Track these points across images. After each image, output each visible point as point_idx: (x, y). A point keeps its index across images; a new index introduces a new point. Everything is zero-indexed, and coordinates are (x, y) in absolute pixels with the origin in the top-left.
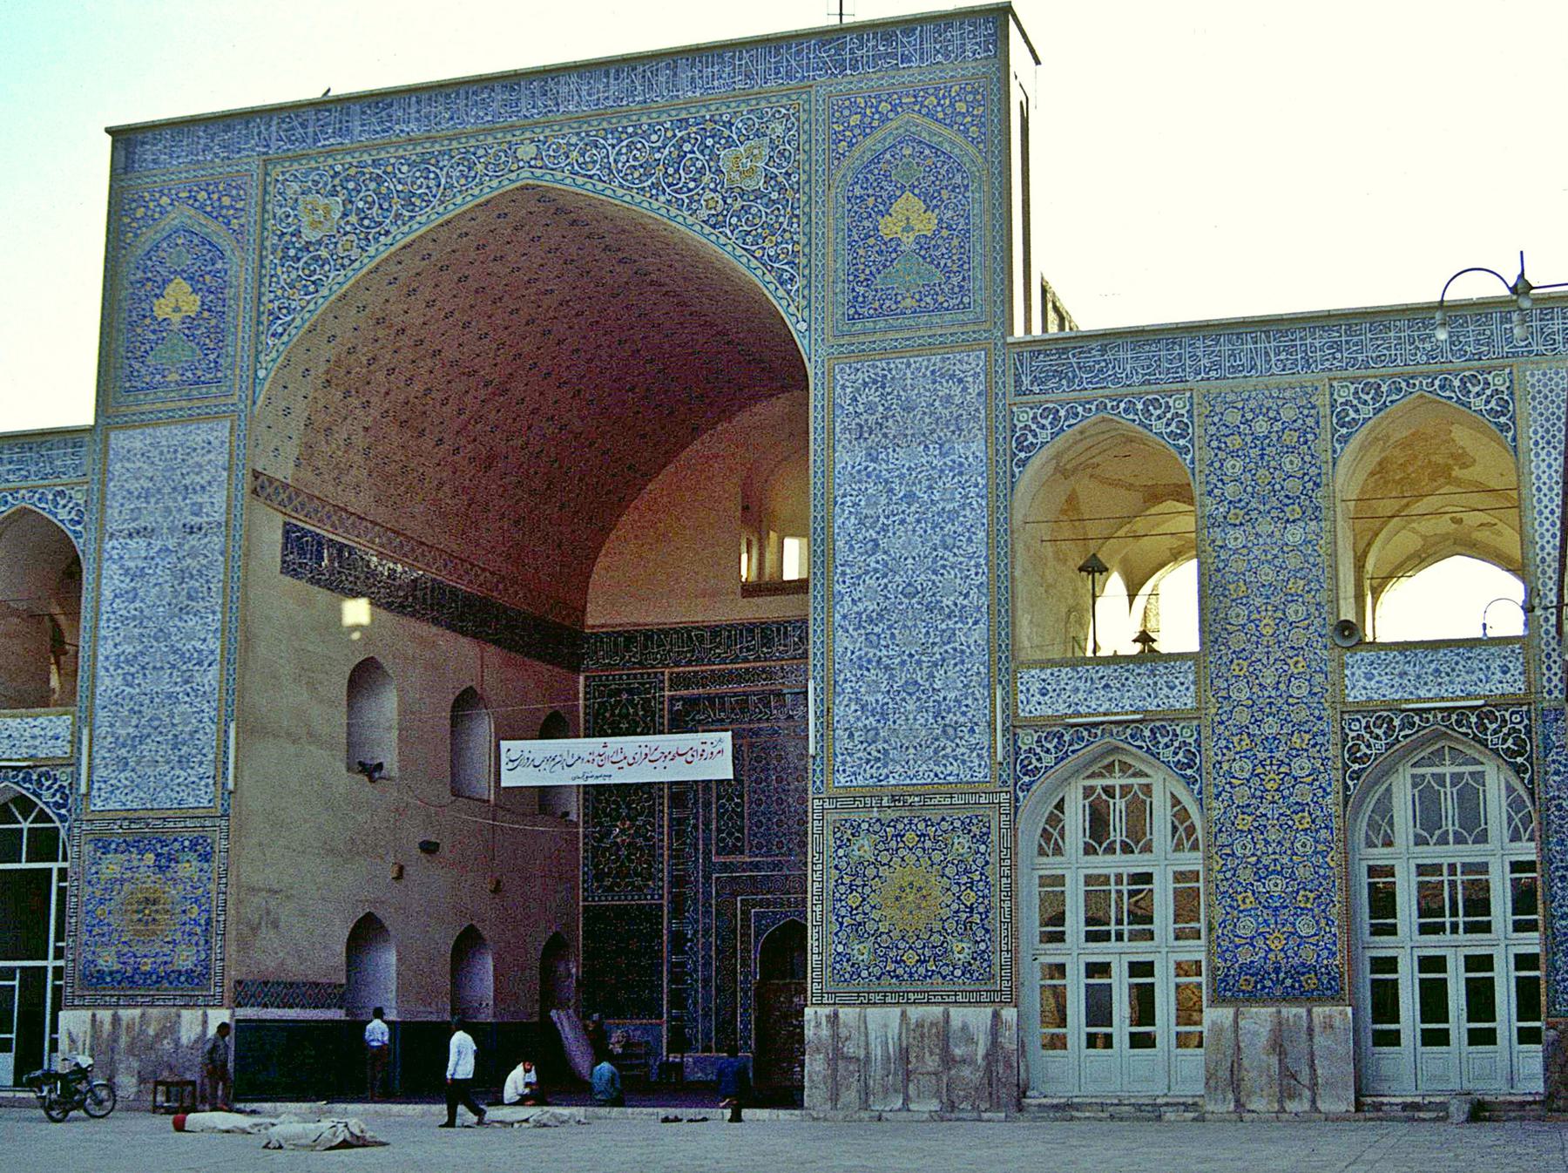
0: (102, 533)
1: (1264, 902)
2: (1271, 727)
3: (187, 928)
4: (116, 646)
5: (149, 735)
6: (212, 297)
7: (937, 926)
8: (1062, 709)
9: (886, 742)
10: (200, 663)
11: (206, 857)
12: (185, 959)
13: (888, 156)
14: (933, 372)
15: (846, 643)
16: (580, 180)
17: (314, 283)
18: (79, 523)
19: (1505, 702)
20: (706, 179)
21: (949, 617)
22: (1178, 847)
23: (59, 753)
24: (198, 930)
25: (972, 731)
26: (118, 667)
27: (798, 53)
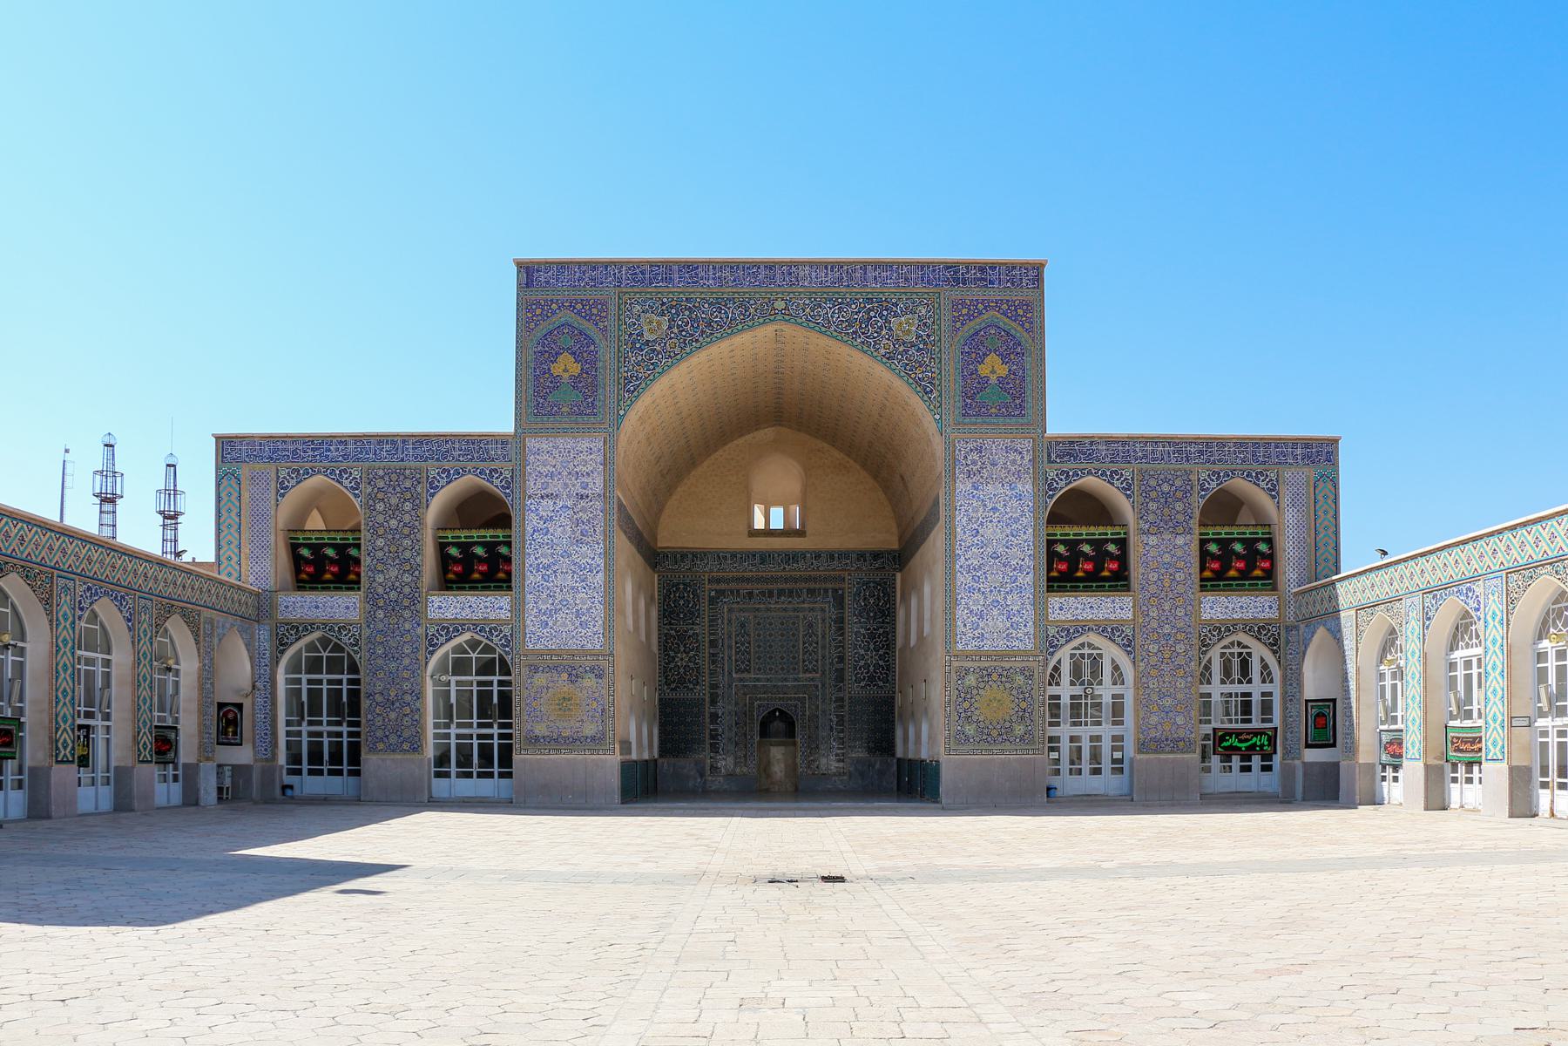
0: (525, 496)
1: (1161, 709)
2: (1167, 629)
8: (1070, 617)
11: (599, 676)
12: (590, 729)
19: (1269, 622)
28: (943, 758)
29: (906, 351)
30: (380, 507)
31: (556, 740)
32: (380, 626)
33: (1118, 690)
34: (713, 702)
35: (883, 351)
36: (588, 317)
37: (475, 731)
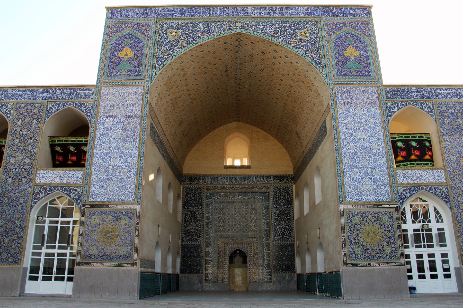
3: (124, 241)
4: (100, 150)
5: (111, 178)
7: (380, 243)
8: (410, 181)
9: (360, 189)
10: (130, 157)
11: (131, 218)
12: (123, 251)
13: (344, 37)
14: (363, 91)
15: (346, 161)
16: (255, 33)
17: (171, 51)
18: (89, 113)
20: (293, 36)
21: (375, 155)
22: (438, 221)
23: (78, 182)
24: (128, 242)
25: (385, 187)
26: (101, 156)
27: (316, 9)
28: (342, 269)
29: (305, 45)
30: (20, 122)
31: (102, 257)
32: (8, 187)
33: (440, 225)
34: (207, 246)
35: (293, 45)
36: (140, 31)
37: (56, 251)
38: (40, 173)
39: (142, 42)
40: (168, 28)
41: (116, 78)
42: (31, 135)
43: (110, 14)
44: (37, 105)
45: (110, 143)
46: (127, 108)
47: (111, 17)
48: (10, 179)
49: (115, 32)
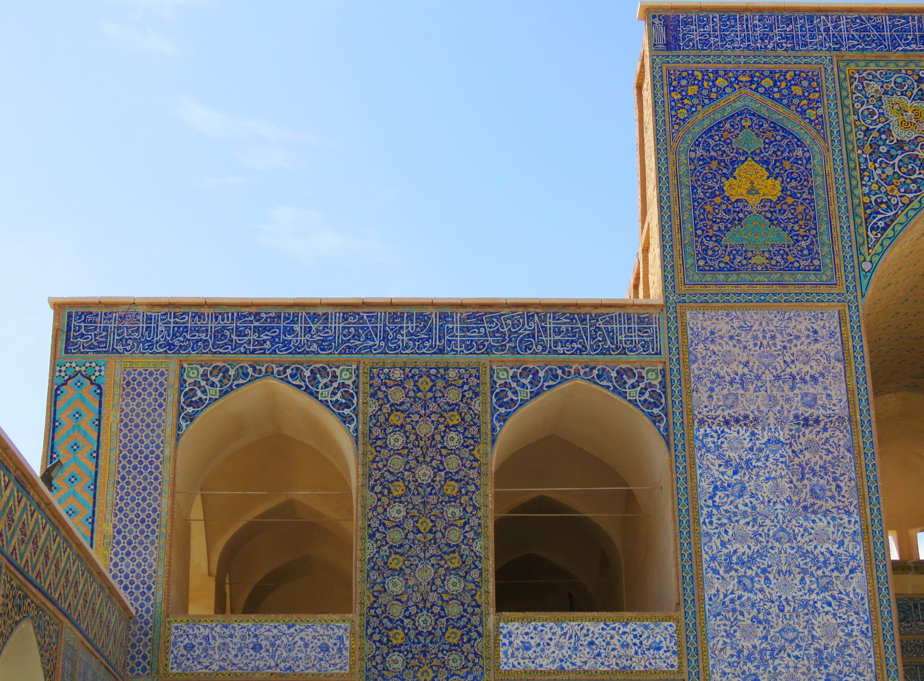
4: (723, 544)
5: (783, 649)
6: (794, 184)
17: (914, 181)
30: (396, 440)
36: (786, 100)
38: (510, 634)
39: (800, 143)
40: (886, 93)
41: (733, 277)
42: (451, 488)
43: (662, 31)
44: (452, 374)
45: (755, 520)
46: (792, 388)
47: (668, 46)
48: (396, 656)
49: (696, 101)
